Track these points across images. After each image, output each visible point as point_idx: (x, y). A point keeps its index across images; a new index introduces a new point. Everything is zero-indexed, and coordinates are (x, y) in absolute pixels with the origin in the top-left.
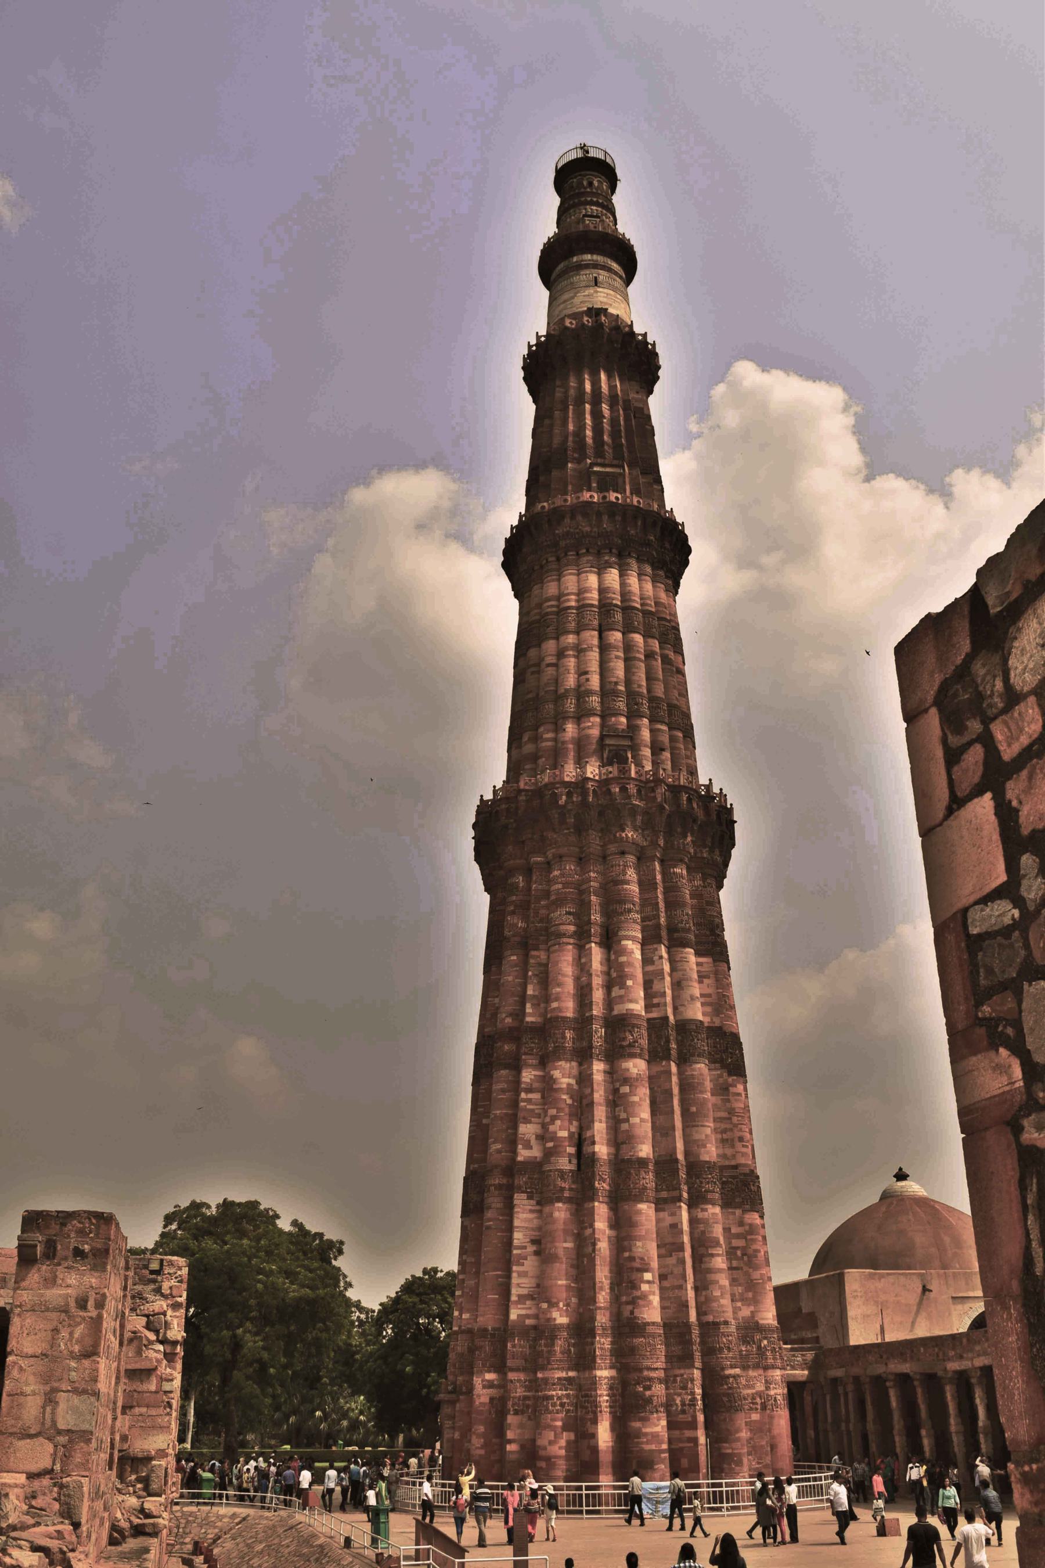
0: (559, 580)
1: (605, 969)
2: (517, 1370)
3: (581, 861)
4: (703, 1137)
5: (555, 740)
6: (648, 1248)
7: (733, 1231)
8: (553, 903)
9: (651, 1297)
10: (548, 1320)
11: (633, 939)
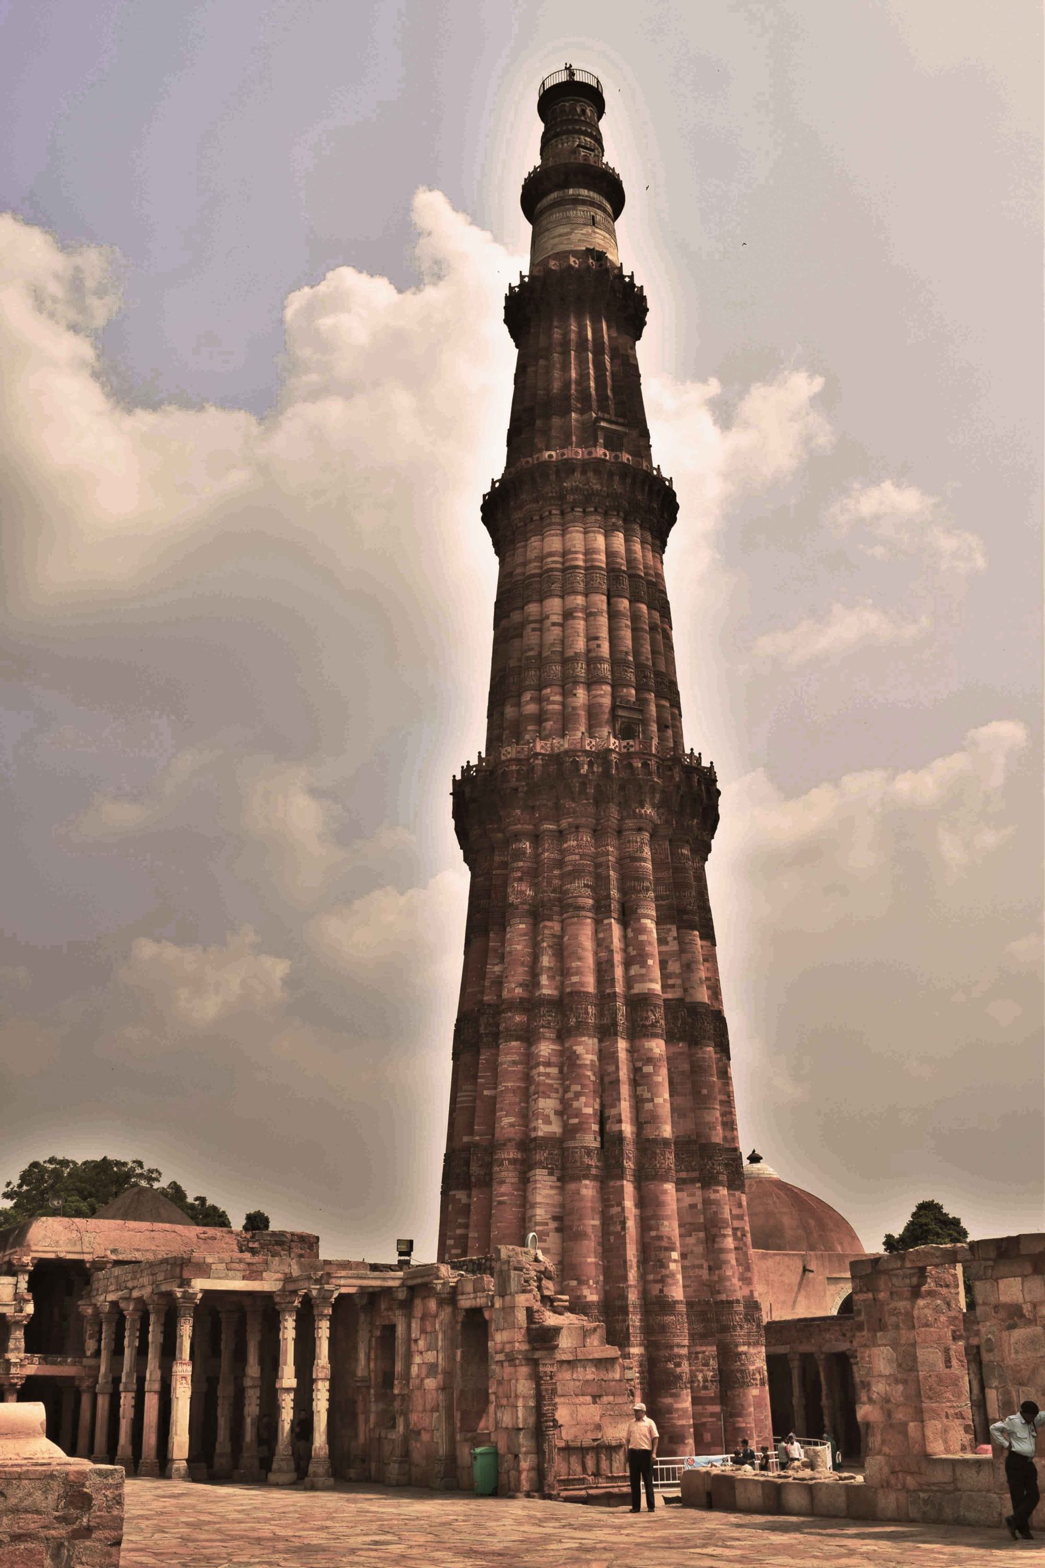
0: (563, 535)
1: (622, 946)
3: (598, 833)
6: (671, 1228)
8: (570, 873)
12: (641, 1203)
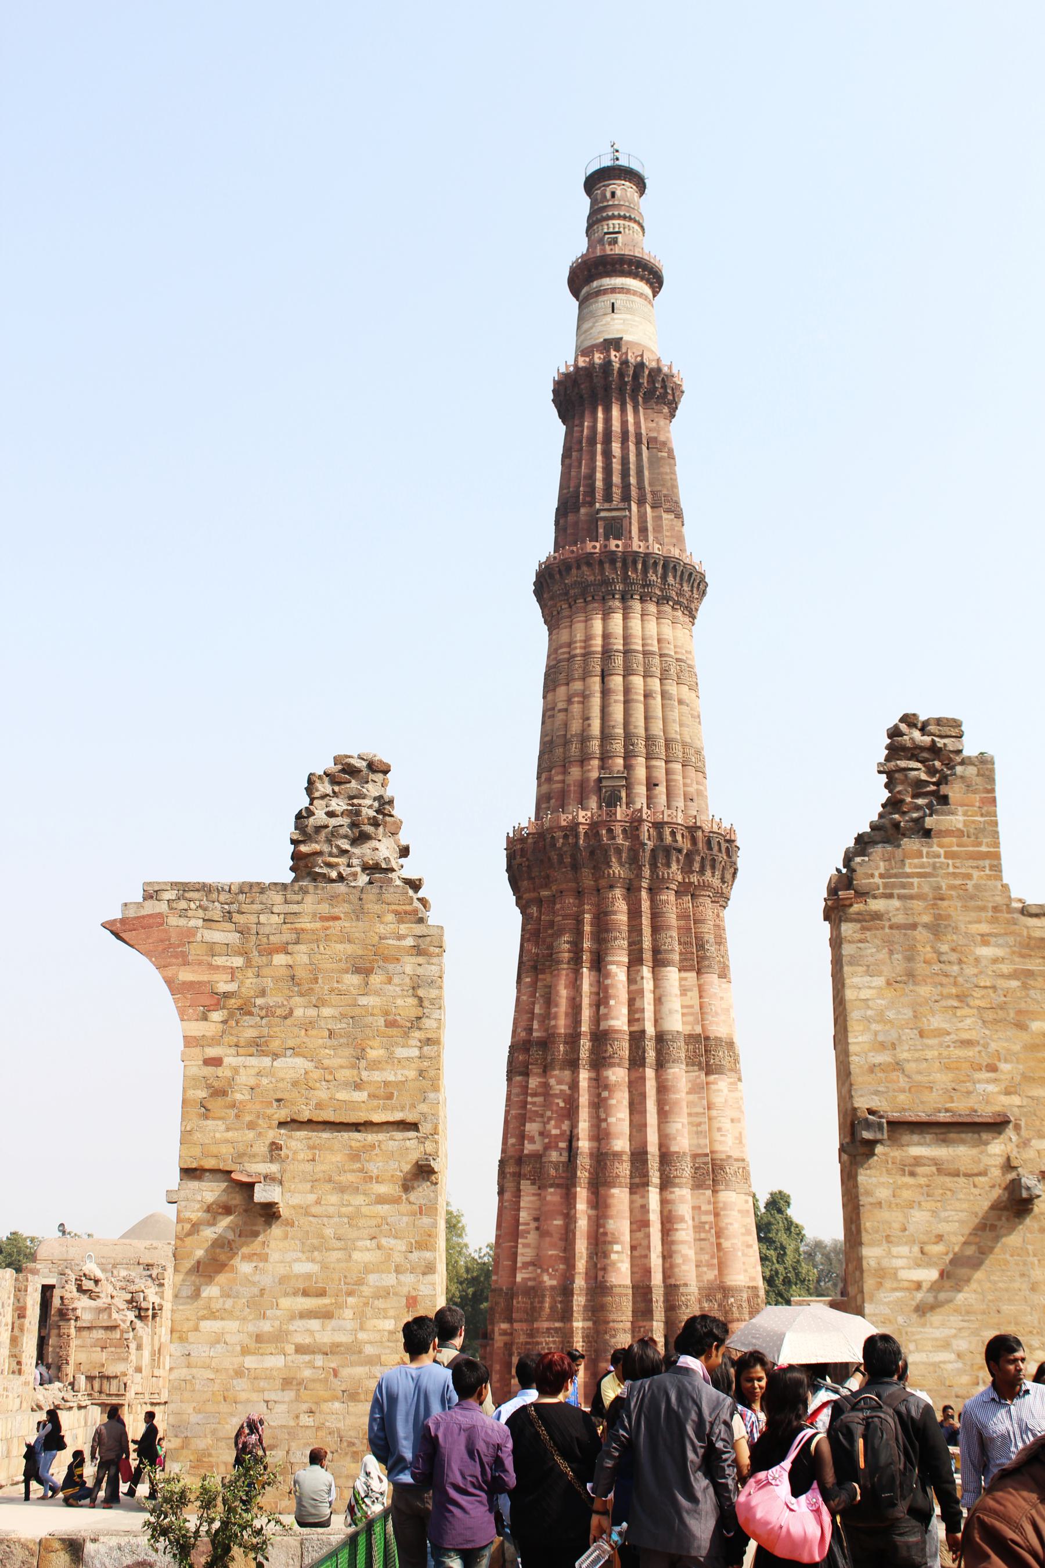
1: (594, 990)
2: (521, 1321)
3: (579, 894)
4: (674, 1132)
5: (563, 782)
6: (620, 1225)
7: (703, 1208)
9: (619, 1265)
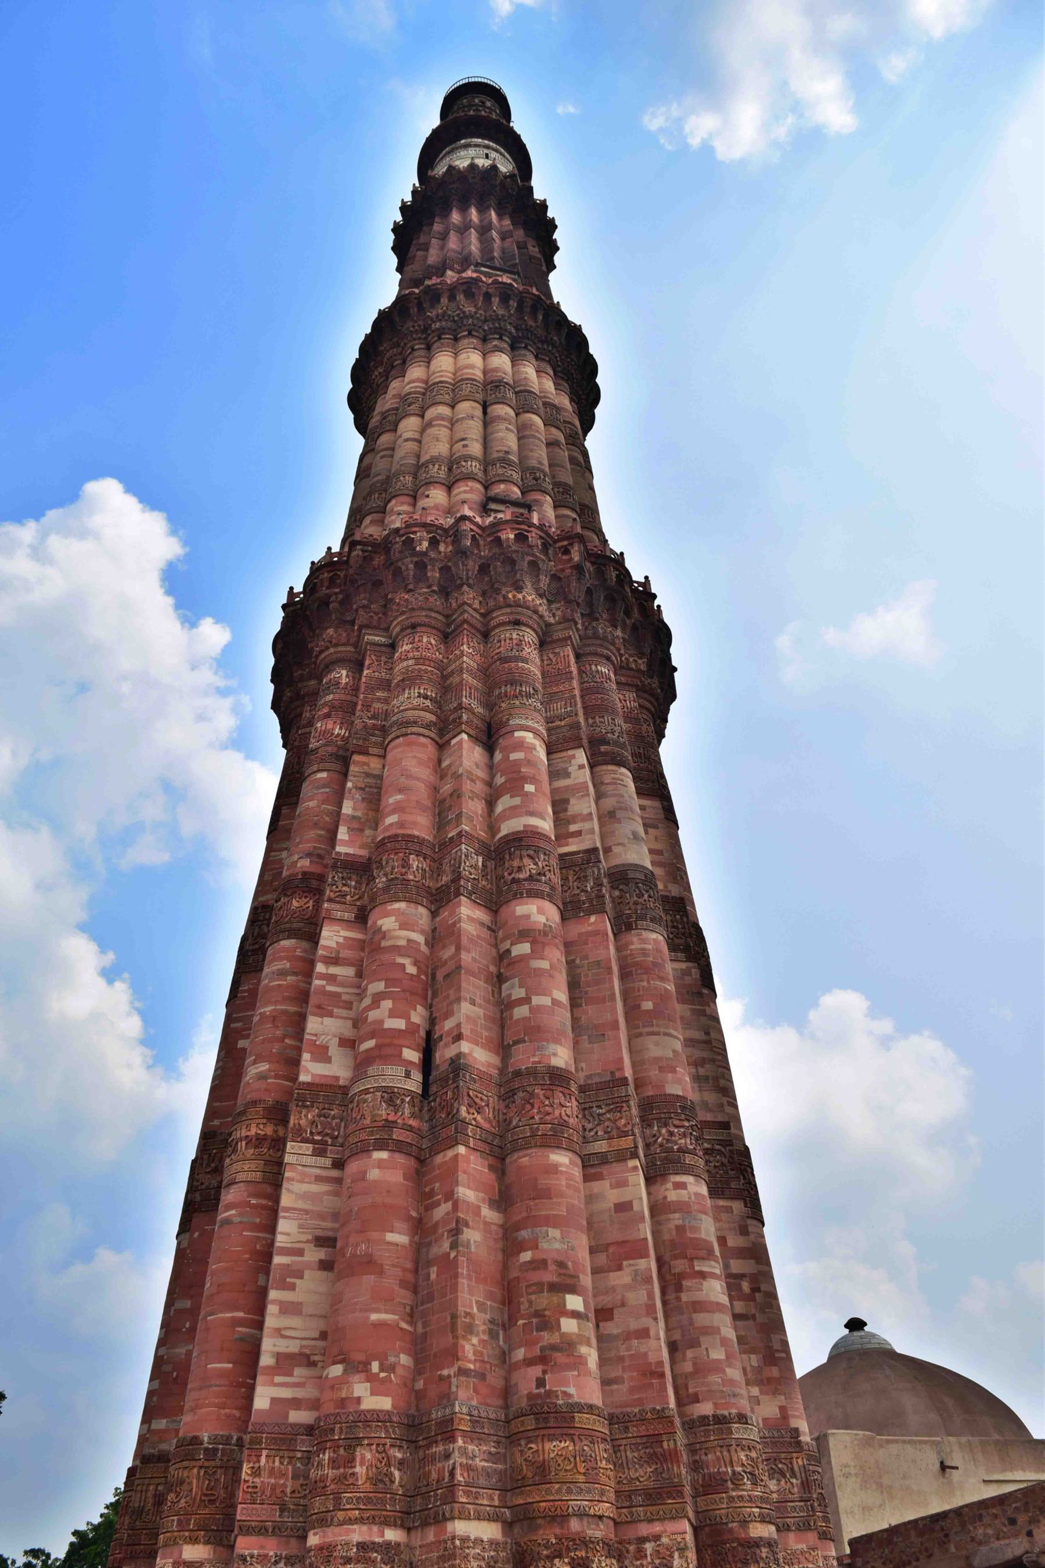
1: (481, 774)
2: (261, 1530)
3: (447, 637)
7: (731, 1243)
9: (584, 1350)
10: (343, 1402)
11: (536, 733)
12: (503, 1199)
